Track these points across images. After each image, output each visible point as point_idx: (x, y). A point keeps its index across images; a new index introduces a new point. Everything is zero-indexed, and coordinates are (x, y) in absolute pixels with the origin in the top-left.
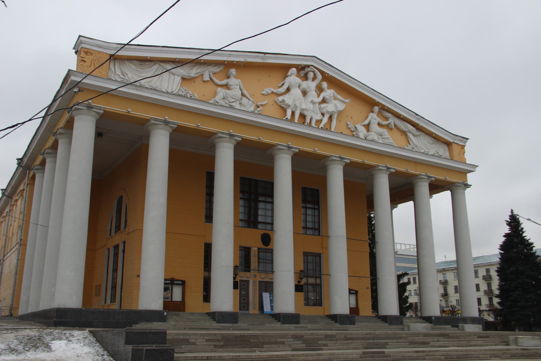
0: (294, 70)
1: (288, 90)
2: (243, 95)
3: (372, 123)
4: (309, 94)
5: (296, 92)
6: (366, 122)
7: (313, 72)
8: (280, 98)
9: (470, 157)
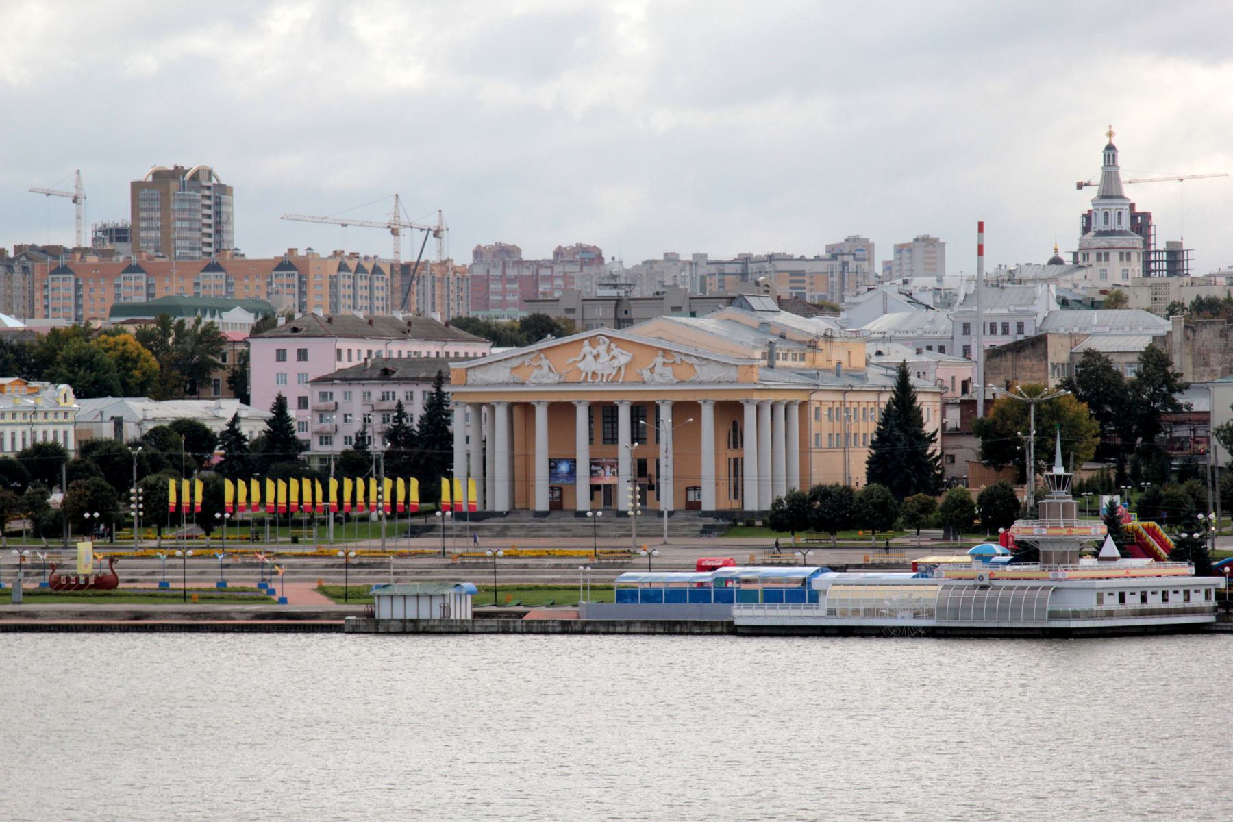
5: (590, 358)
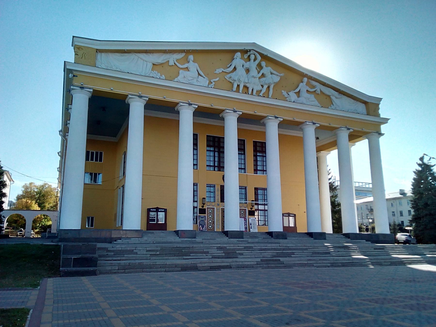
0: (239, 54)
1: (235, 68)
2: (199, 74)
3: (301, 91)
4: (251, 72)
5: (241, 71)
6: (297, 90)
7: (254, 54)
8: (229, 76)
9: (383, 112)
